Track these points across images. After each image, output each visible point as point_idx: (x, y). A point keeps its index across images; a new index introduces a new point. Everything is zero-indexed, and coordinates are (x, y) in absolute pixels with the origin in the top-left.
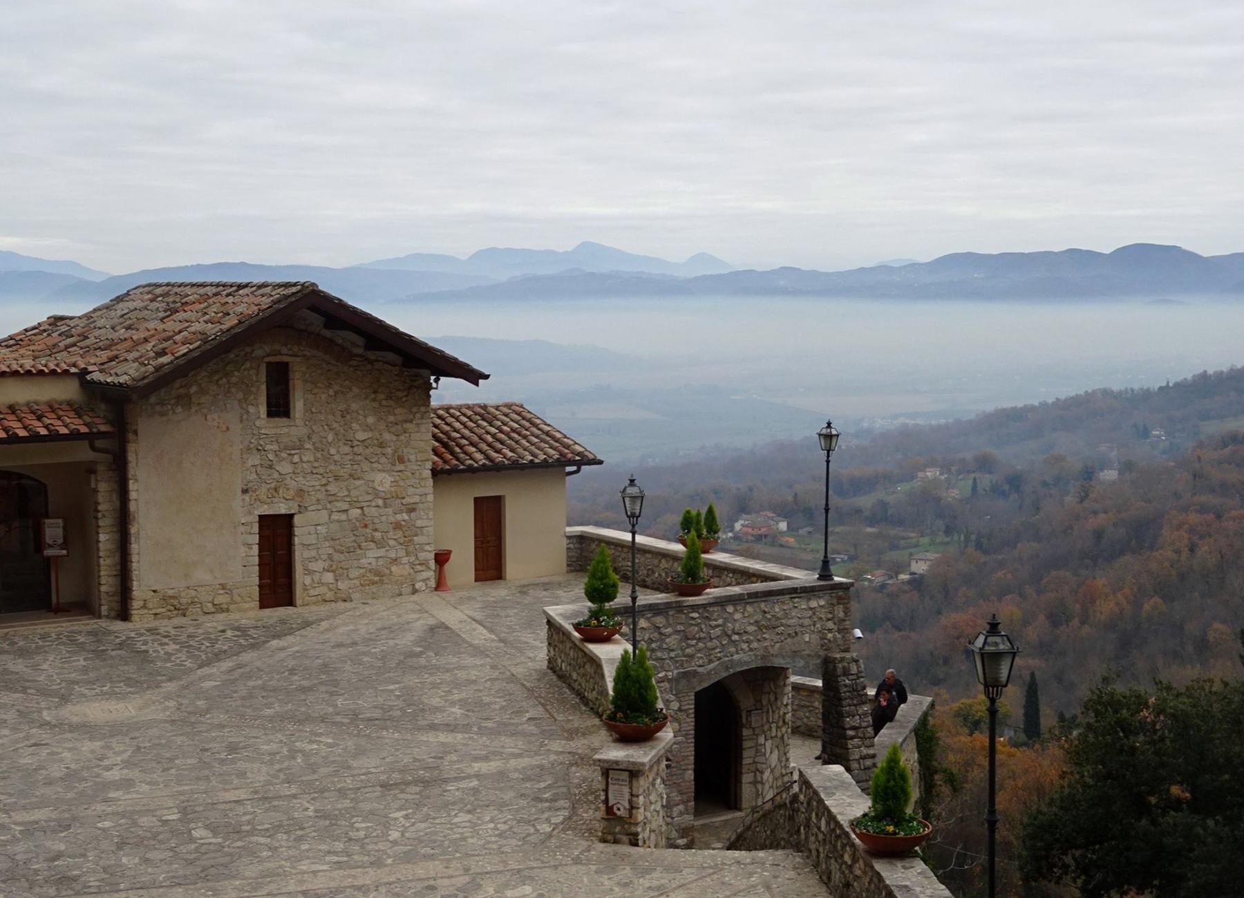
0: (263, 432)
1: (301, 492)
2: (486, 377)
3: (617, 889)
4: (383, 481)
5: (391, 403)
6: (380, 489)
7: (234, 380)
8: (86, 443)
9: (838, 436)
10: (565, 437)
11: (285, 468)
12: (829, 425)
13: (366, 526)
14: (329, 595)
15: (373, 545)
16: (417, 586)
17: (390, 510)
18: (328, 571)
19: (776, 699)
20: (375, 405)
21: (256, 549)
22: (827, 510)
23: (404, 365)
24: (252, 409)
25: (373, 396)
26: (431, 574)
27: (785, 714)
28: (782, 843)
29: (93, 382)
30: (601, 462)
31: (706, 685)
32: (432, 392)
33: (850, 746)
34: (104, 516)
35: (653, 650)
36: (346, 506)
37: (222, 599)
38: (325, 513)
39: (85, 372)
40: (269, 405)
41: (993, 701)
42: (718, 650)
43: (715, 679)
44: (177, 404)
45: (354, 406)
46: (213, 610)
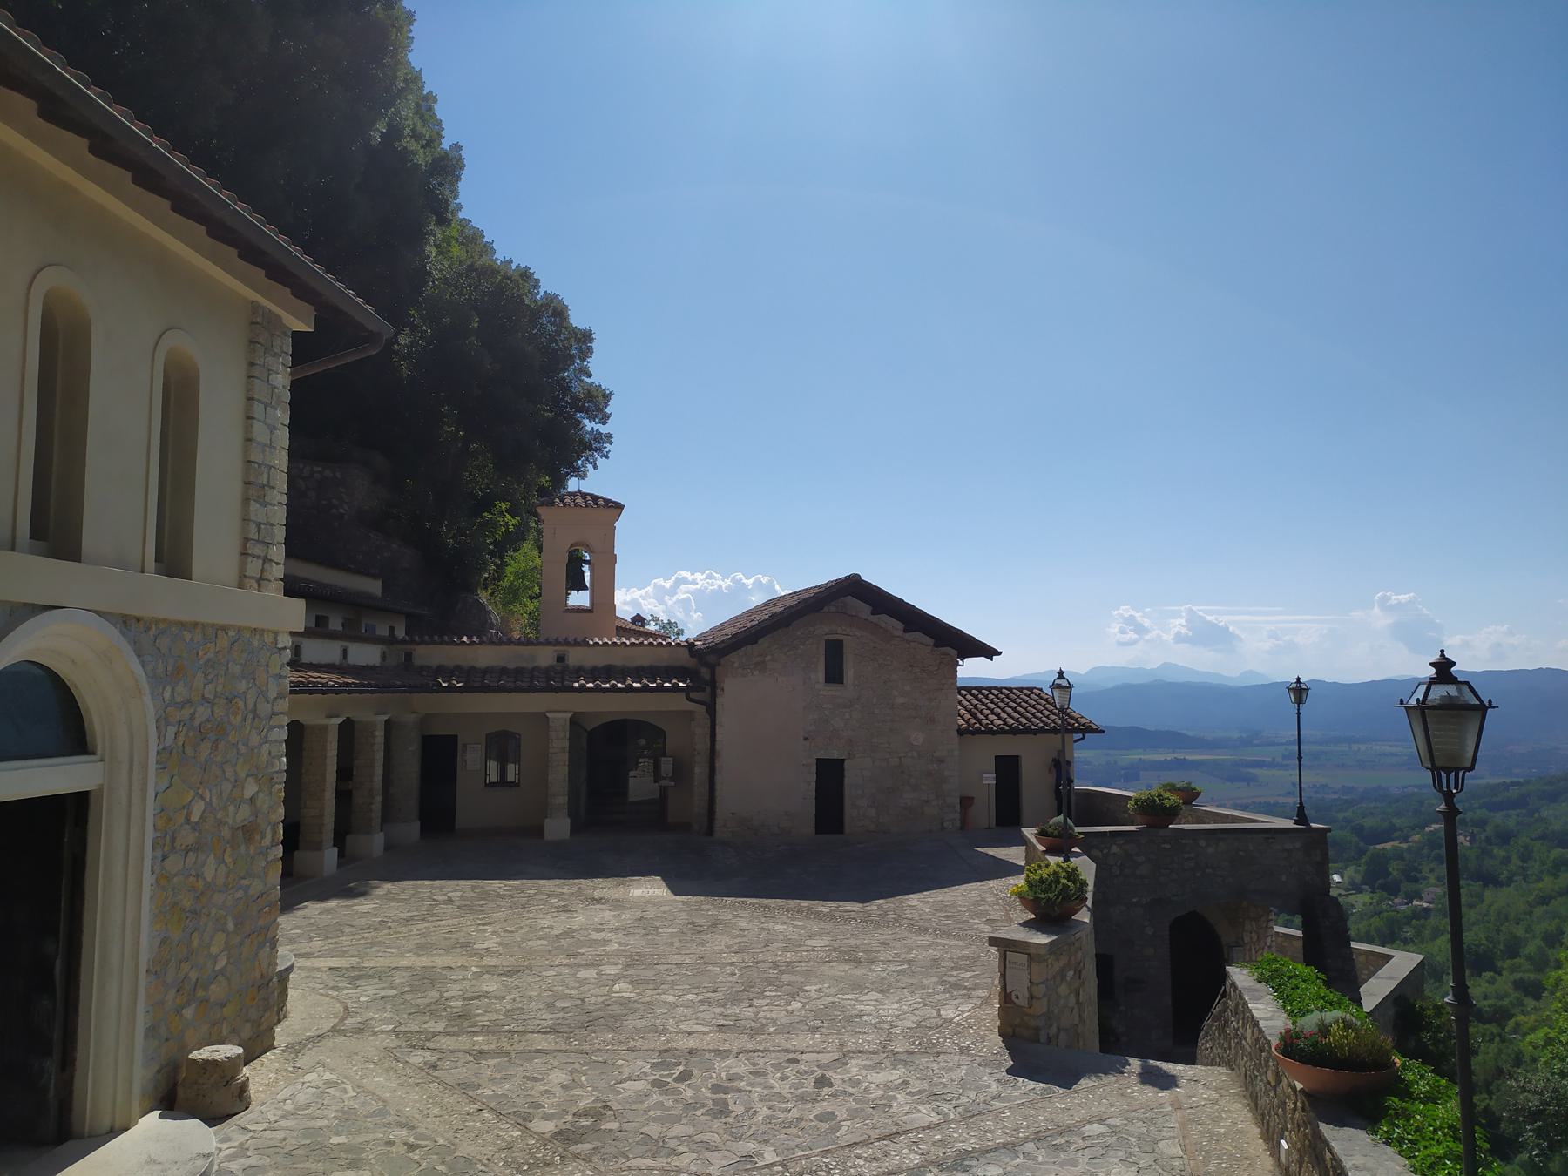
0: (821, 693)
2: (1000, 653)
3: (994, 1086)
6: (915, 743)
8: (684, 694)
9: (1308, 689)
10: (1075, 712)
13: (902, 772)
16: (945, 825)
21: (814, 784)
22: (1300, 758)
23: (936, 645)
25: (910, 669)
26: (957, 816)
28: (821, 915)
30: (1103, 732)
32: (958, 668)
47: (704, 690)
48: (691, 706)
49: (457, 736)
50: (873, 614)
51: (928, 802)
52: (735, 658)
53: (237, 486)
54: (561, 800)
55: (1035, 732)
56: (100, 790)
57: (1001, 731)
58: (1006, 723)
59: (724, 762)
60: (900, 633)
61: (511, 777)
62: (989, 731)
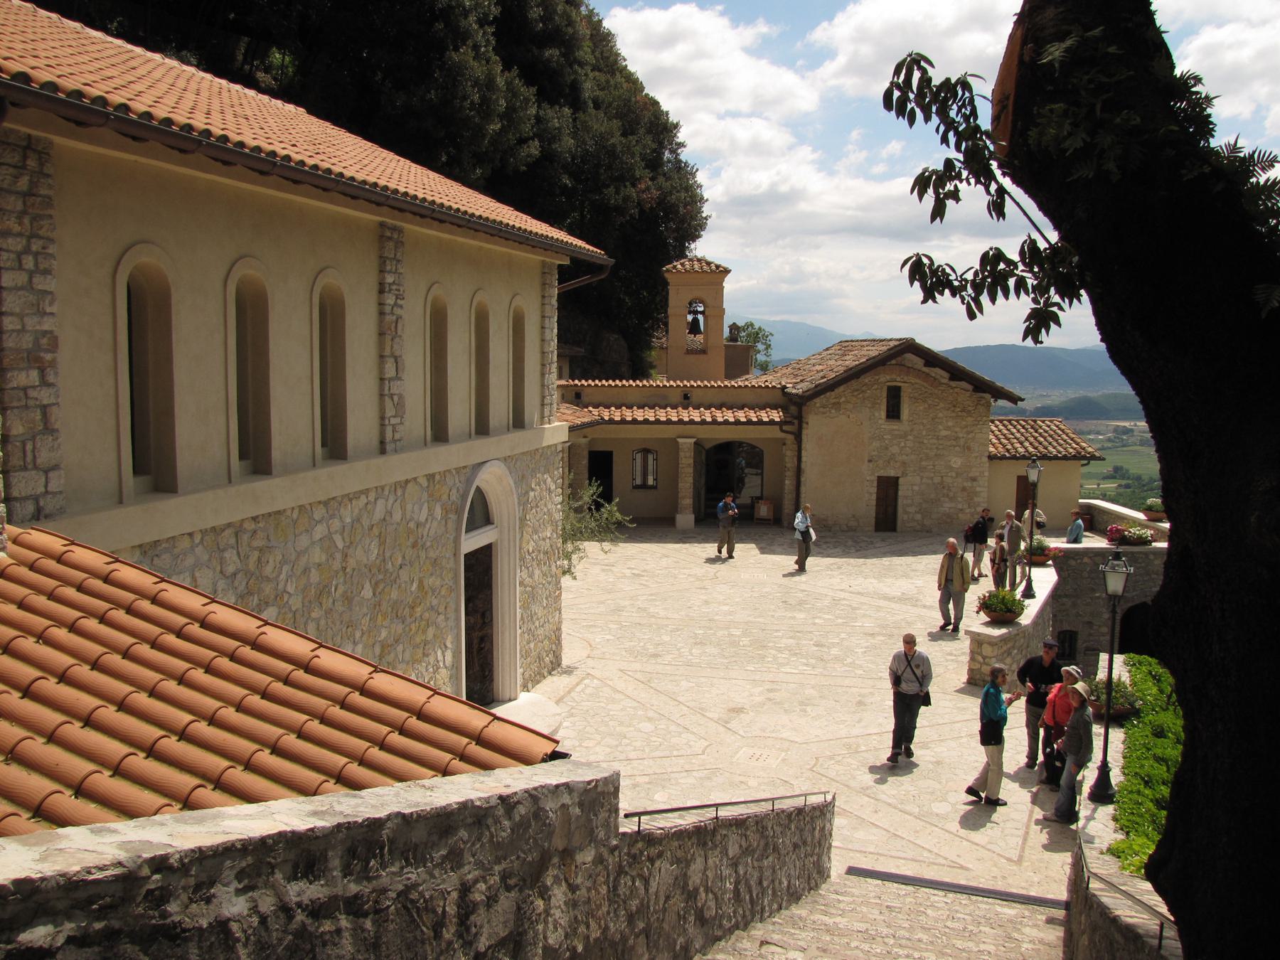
1: (904, 463)
2: (1022, 400)
4: (956, 462)
5: (965, 414)
7: (867, 395)
11: (895, 449)
13: (943, 488)
14: (918, 527)
15: (947, 499)
17: (960, 480)
18: (918, 513)
20: (954, 414)
21: (874, 497)
23: (974, 391)
24: (877, 414)
29: (790, 394)
31: (1130, 605)
34: (789, 470)
35: (1092, 579)
36: (932, 475)
37: (852, 523)
38: (918, 478)
39: (785, 387)
40: (888, 411)
43: (1138, 602)
44: (832, 408)
45: (940, 415)
46: (845, 527)
47: (793, 424)
48: (783, 435)
49: (611, 453)
50: (926, 365)
51: (962, 510)
52: (818, 401)
53: (539, 367)
54: (687, 501)
55: (1050, 459)
56: (497, 540)
57: (1023, 457)
58: (1027, 451)
59: (809, 477)
60: (945, 381)
61: (651, 481)
62: (1014, 458)
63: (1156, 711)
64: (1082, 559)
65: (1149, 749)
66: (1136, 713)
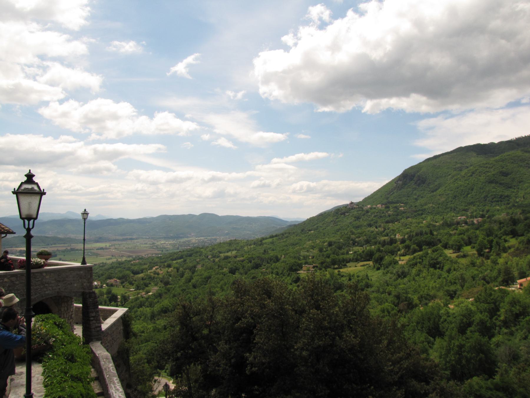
12: (85, 210)
19: (68, 309)
27: (71, 315)
33: (91, 323)
41: (29, 230)
42: (39, 290)
63: (65, 345)
64: (3, 280)
65: (66, 373)
66: (50, 348)
